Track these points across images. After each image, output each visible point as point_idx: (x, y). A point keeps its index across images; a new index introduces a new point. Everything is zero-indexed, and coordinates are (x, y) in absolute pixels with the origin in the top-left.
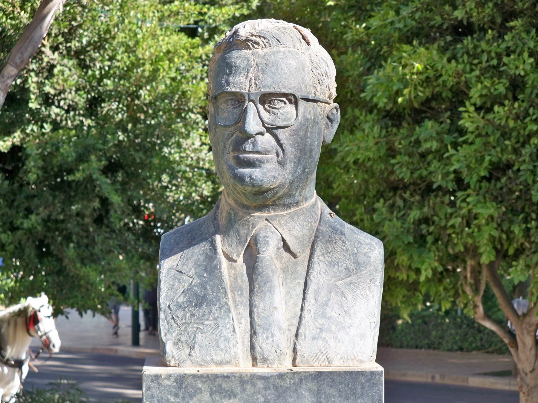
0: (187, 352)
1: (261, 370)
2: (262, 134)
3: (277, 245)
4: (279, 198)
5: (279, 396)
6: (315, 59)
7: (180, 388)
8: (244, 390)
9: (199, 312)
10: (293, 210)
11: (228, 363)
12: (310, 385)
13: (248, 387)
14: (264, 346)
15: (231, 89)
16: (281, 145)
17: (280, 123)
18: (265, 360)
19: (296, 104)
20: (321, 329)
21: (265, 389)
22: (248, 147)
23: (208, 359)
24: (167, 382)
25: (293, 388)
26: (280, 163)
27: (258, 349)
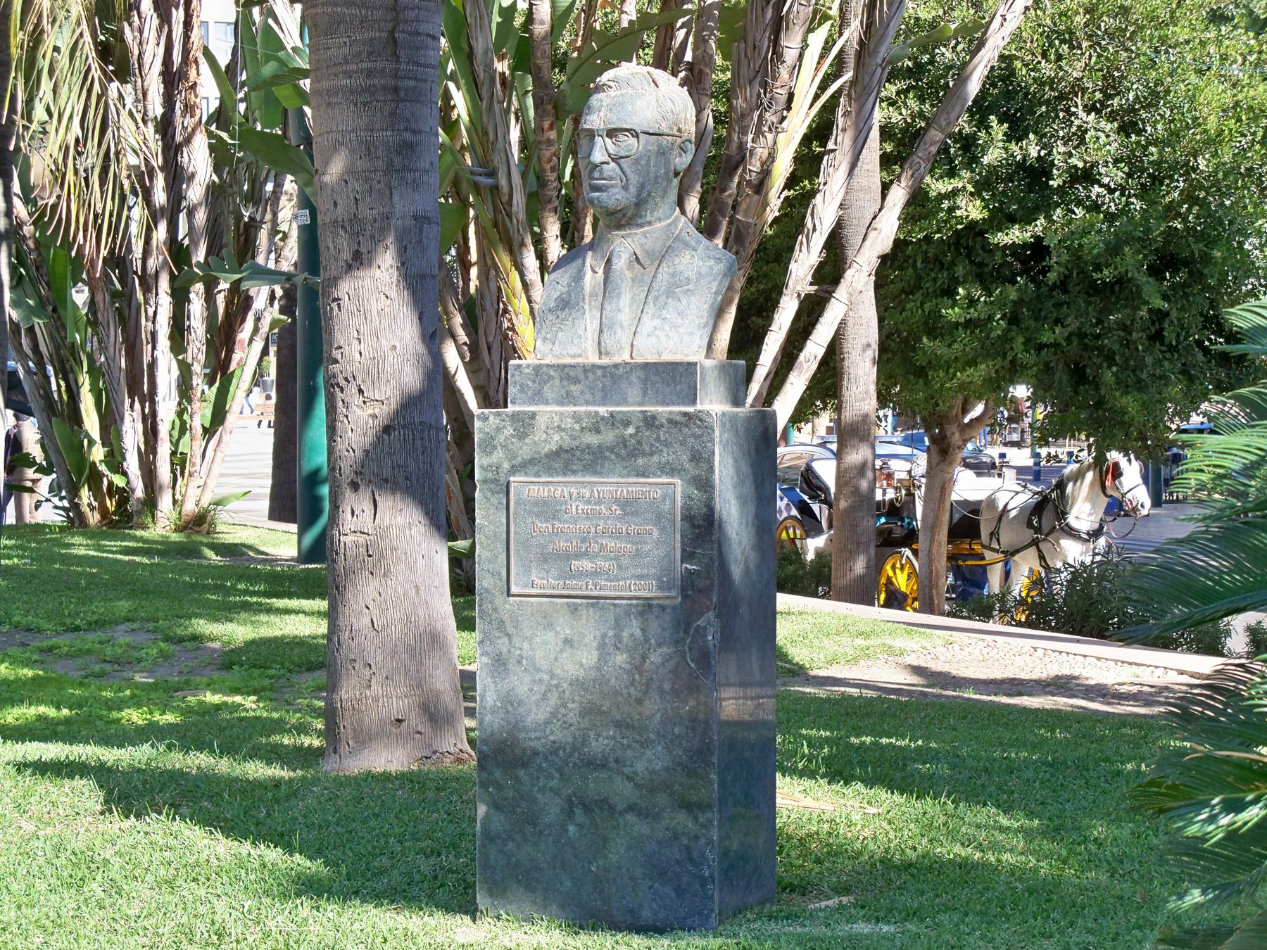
0: (550, 347)
1: (605, 361)
2: (607, 163)
3: (629, 258)
4: (630, 219)
5: (614, 383)
6: (661, 99)
7: (537, 376)
8: (587, 377)
9: (562, 315)
10: (646, 229)
11: (580, 356)
12: (638, 373)
13: (590, 374)
14: (608, 341)
15: (586, 126)
16: (624, 173)
17: (623, 154)
18: (607, 353)
19: (637, 136)
20: (655, 328)
21: (604, 376)
22: (596, 175)
23: (565, 353)
24: (527, 371)
25: (625, 376)
26: (623, 187)
27: (603, 344)
